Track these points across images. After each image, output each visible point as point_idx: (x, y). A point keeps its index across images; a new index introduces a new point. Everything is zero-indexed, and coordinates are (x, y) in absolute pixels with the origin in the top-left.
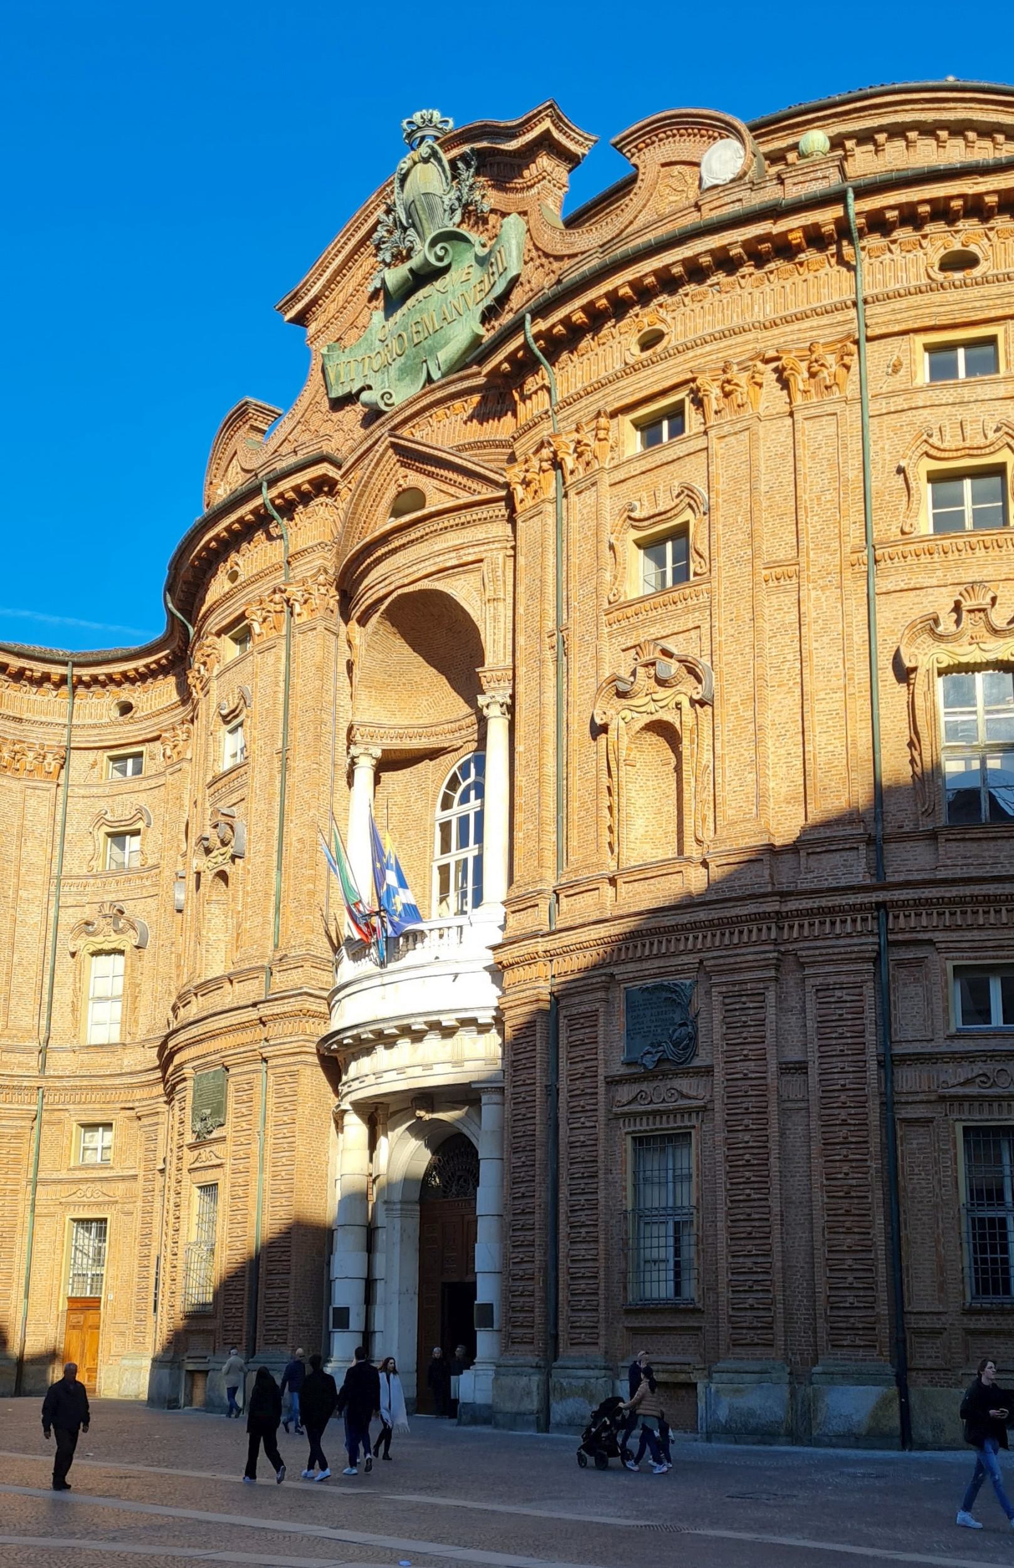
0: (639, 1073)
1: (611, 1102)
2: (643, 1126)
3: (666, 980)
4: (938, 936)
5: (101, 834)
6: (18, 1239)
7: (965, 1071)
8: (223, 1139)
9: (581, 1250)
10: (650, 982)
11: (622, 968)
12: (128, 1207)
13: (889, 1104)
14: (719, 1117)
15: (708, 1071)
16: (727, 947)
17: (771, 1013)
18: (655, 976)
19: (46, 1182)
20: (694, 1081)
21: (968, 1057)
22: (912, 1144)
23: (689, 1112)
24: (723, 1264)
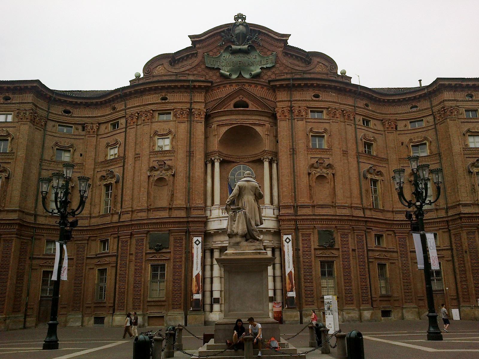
0: (322, 248)
1: (315, 253)
3: (328, 229)
4: (373, 228)
8: (170, 252)
9: (308, 284)
10: (324, 229)
11: (317, 225)
14: (341, 259)
15: (338, 249)
16: (341, 225)
17: (350, 239)
18: (325, 228)
20: (335, 251)
21: (378, 251)
22: (371, 265)
23: (334, 257)
24: (343, 288)
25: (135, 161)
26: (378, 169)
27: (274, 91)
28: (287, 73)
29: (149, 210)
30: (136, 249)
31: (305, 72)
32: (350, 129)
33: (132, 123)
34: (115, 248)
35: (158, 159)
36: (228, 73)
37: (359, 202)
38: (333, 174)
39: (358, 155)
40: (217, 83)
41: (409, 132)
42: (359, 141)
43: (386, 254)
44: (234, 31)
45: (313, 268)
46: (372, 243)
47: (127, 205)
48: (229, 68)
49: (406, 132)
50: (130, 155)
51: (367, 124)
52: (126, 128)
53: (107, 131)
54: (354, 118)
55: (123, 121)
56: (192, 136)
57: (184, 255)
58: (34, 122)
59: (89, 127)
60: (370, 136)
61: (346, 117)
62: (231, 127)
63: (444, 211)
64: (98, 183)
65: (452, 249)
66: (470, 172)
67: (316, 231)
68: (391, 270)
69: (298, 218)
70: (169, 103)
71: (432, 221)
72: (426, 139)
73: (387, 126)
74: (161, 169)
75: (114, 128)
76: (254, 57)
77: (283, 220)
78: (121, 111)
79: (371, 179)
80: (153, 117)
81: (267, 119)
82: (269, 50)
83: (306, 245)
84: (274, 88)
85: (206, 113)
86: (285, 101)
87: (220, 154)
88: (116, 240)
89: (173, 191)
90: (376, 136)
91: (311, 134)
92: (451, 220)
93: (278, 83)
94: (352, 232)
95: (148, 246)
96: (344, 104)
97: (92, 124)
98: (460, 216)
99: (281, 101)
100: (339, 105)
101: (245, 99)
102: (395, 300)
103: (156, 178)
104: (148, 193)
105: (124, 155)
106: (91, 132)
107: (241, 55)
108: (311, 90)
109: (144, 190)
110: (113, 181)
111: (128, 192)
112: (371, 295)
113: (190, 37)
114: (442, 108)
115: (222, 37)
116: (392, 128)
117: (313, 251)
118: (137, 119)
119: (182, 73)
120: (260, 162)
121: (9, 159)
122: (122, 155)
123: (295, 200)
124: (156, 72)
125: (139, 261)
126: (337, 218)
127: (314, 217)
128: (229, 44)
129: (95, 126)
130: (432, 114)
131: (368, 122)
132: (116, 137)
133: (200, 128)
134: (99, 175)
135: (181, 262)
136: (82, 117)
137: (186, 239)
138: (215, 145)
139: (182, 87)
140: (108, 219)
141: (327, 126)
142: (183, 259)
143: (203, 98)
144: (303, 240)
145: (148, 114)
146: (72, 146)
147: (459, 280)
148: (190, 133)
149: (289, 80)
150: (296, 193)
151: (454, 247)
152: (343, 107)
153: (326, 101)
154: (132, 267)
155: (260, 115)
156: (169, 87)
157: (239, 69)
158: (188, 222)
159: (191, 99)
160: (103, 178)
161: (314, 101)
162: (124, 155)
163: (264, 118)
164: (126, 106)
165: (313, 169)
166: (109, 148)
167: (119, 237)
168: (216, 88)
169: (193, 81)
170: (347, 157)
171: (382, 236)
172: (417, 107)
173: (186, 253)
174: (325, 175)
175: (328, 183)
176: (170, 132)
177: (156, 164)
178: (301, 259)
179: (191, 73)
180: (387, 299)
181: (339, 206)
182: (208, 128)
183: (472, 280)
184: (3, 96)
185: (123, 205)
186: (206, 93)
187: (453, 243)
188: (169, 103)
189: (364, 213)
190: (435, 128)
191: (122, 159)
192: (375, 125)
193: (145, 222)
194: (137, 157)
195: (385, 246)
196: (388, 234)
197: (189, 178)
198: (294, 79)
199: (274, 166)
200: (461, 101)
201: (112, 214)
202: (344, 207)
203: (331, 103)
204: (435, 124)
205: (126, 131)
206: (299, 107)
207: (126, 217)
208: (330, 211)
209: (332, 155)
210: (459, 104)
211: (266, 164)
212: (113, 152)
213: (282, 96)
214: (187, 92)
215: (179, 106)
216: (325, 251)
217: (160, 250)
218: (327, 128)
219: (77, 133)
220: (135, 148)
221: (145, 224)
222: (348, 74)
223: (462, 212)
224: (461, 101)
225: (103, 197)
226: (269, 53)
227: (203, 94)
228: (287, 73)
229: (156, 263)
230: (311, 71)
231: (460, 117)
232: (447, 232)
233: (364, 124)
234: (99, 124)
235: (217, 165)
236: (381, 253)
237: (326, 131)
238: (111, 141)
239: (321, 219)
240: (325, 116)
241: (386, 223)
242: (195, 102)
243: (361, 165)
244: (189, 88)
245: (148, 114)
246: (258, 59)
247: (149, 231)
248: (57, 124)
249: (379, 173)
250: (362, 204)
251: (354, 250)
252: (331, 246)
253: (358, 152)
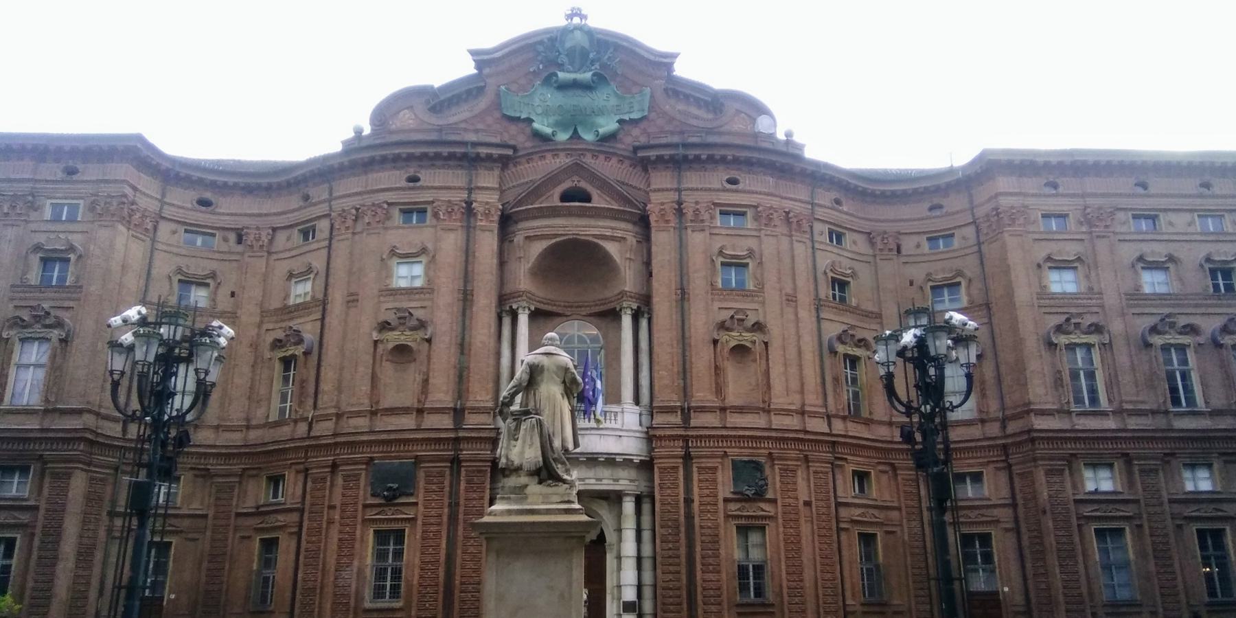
2: (743, 522)
3: (754, 459)
5: (175, 279)
7: (859, 511)
8: (416, 504)
10: (746, 459)
12: (190, 536)
14: (780, 521)
15: (774, 501)
17: (800, 480)
22: (844, 536)
23: (765, 518)
25: (348, 308)
26: (860, 334)
27: (645, 170)
28: (672, 133)
29: (373, 413)
30: (343, 495)
31: (710, 131)
32: (801, 251)
33: (343, 228)
34: (299, 492)
35: (397, 305)
36: (549, 131)
37: (820, 402)
38: (766, 344)
39: (819, 306)
40: (525, 148)
41: (926, 258)
42: (820, 276)
43: (876, 512)
44: (562, 42)
45: (722, 542)
46: (846, 489)
47: (327, 401)
48: (552, 120)
49: (919, 259)
50: (337, 298)
51: (839, 241)
52: (331, 239)
53: (289, 245)
54: (811, 227)
55: (324, 225)
56: (470, 259)
57: (446, 510)
58: (129, 222)
59: (252, 237)
60: (845, 266)
61: (794, 226)
62: (554, 241)
63: (997, 425)
64: (268, 355)
65: (1014, 506)
66: (1051, 346)
67: (728, 463)
68: (885, 547)
69: (690, 433)
70: (422, 188)
71: (973, 444)
72: (959, 273)
73: (880, 246)
74: (401, 328)
75: (306, 238)
76: (603, 98)
77: (660, 438)
78: (320, 202)
79: (846, 356)
80: (388, 217)
81: (630, 226)
82: (635, 83)
83: (707, 492)
84: (645, 165)
85: (502, 211)
86: (667, 190)
87: (530, 297)
88: (301, 477)
89: (427, 374)
90: (857, 266)
91: (721, 259)
92: (1013, 444)
93: (652, 154)
94: (804, 466)
95: (369, 489)
96: (791, 199)
97: (258, 228)
98: (1031, 438)
99: (659, 190)
101: (583, 184)
102: (895, 613)
103: (390, 346)
104: (373, 378)
105: (325, 295)
106: (256, 245)
107: (579, 92)
108: (721, 168)
109: (364, 371)
110: (299, 351)
111: (328, 375)
112: (844, 601)
113: (474, 53)
114: (993, 209)
115: (539, 53)
116: (890, 250)
117: (721, 504)
118: (355, 220)
119: (453, 128)
120: (610, 316)
121: (69, 299)
122: (320, 296)
123: (685, 395)
124: (395, 124)
125: (348, 521)
126: (774, 434)
127: (725, 433)
128: (552, 70)
129: (264, 234)
130: (974, 222)
131: (840, 237)
132: (309, 258)
133: (487, 243)
134: (270, 338)
135: (439, 524)
136: (236, 215)
137: (451, 475)
138: (522, 278)
139: (452, 156)
140: (286, 431)
141: (752, 243)
142: (445, 518)
143: (497, 180)
144: (700, 481)
145: (379, 211)
146: (213, 275)
147: (1030, 572)
148: (468, 253)
149: (676, 146)
150: (688, 381)
151: (1020, 501)
152: (788, 205)
153: (753, 192)
154: (334, 535)
155: (616, 219)
156: (424, 156)
157: (573, 121)
158: (457, 440)
159: (471, 181)
160: (277, 344)
161: (728, 190)
162: (325, 295)
163: (623, 225)
164: (331, 194)
165: (722, 333)
166: (294, 280)
167: (307, 470)
168: (523, 160)
169: (475, 144)
170: (796, 307)
171: (867, 474)
172: (940, 207)
173: (450, 505)
174: (748, 344)
175: (755, 361)
176: (424, 251)
177: (391, 317)
178: (697, 520)
179: (471, 127)
180: (877, 609)
181: (776, 409)
182: (506, 244)
183: (1058, 571)
184: (62, 166)
185: (320, 402)
186: (503, 170)
187: (1017, 491)
188: (422, 188)
189: (830, 425)
190: (980, 251)
191: (322, 304)
192: (855, 243)
193: (365, 438)
194: (352, 300)
195: (874, 495)
196: (881, 472)
197: (463, 347)
198: (685, 146)
199: (644, 323)
200: (1033, 195)
201: (296, 421)
202: (787, 412)
204: (979, 244)
205: (329, 247)
206: (697, 203)
207: (324, 428)
208: (759, 421)
209: (763, 303)
210: (1030, 201)
211: (627, 321)
212: (302, 291)
213: (662, 179)
214: (462, 167)
215: (445, 196)
216: (747, 505)
217: (395, 497)
218: (755, 247)
219: (224, 248)
220: (349, 282)
221: (363, 442)
222: (797, 138)
223: (1037, 427)
224: (1033, 195)
225: (277, 385)
226: (635, 90)
227: (497, 172)
228: (672, 133)
229: (384, 527)
230: (722, 129)
231: (1031, 228)
232: (1004, 468)
233: (831, 240)
234: (274, 230)
235: (523, 319)
237: (751, 254)
238: (297, 265)
239: (740, 437)
240: (749, 223)
241: (876, 448)
242: (479, 188)
243: (825, 325)
244: (469, 159)
245: (379, 211)
246: (613, 101)
247: (372, 459)
248: (182, 229)
249: (862, 343)
250: (826, 406)
251: (807, 504)
252: (759, 496)
253: (817, 297)
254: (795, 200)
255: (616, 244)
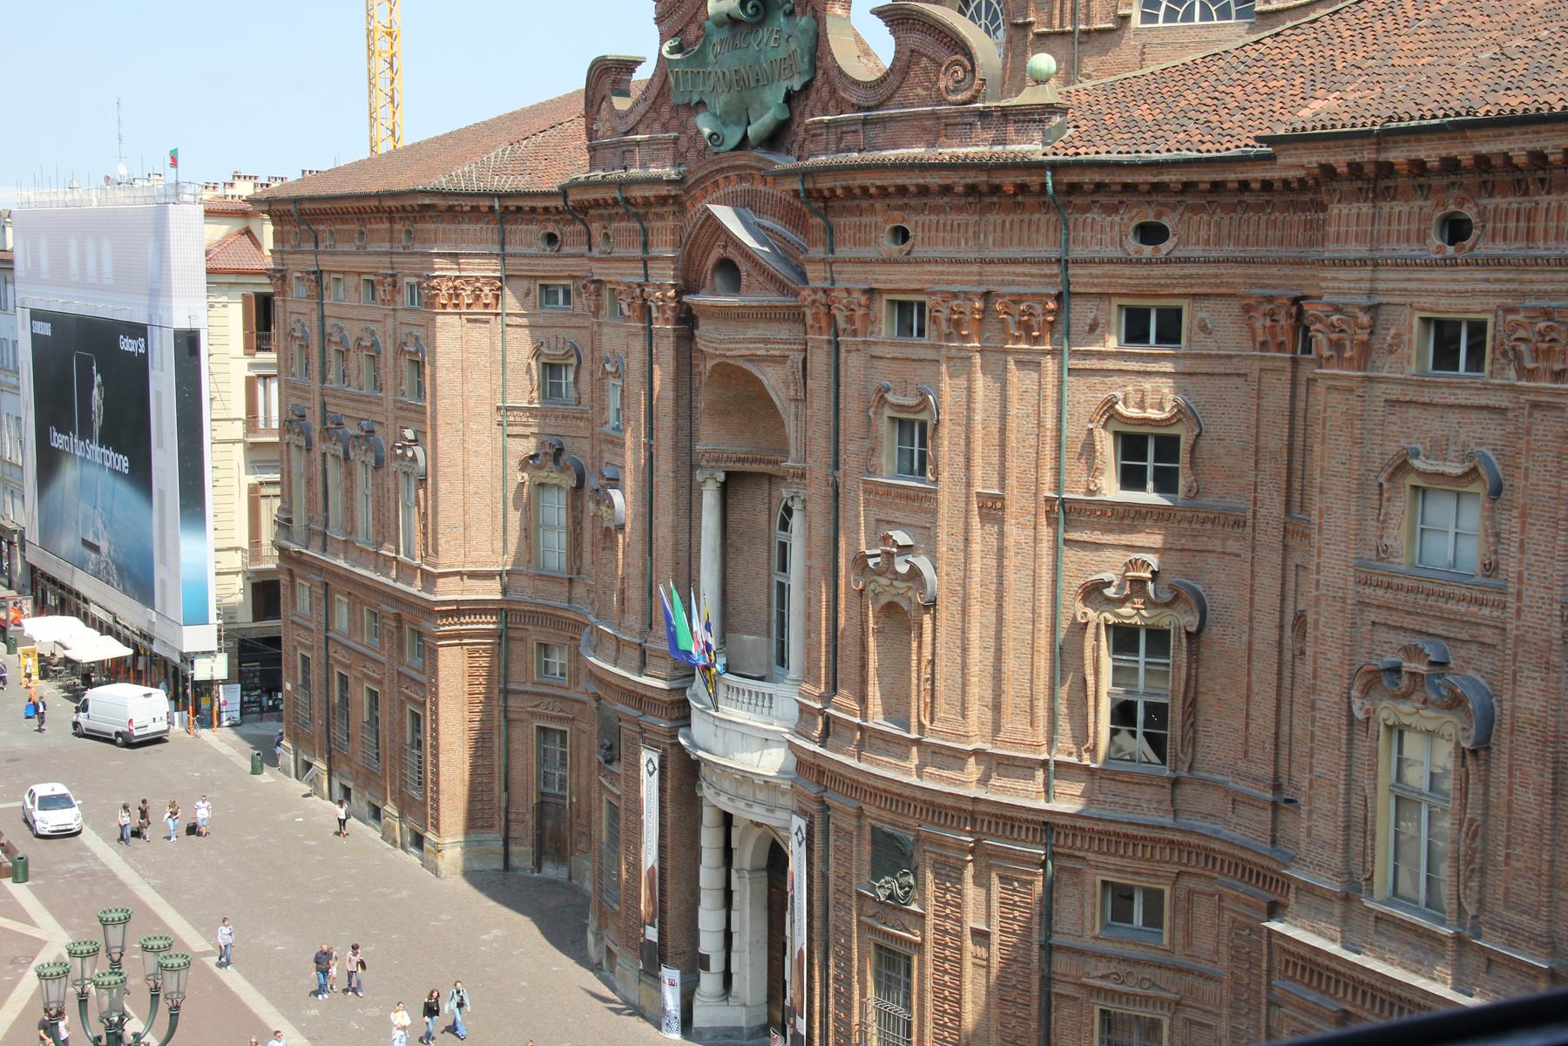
6: (496, 740)
7: (1103, 968)
13: (1047, 980)
19: (515, 692)
21: (1108, 958)
22: (1063, 1015)
100: (975, 268)
203: (940, 268)
236: (1124, 968)
251: (981, 937)
254: (1014, 262)
255: (779, 368)
